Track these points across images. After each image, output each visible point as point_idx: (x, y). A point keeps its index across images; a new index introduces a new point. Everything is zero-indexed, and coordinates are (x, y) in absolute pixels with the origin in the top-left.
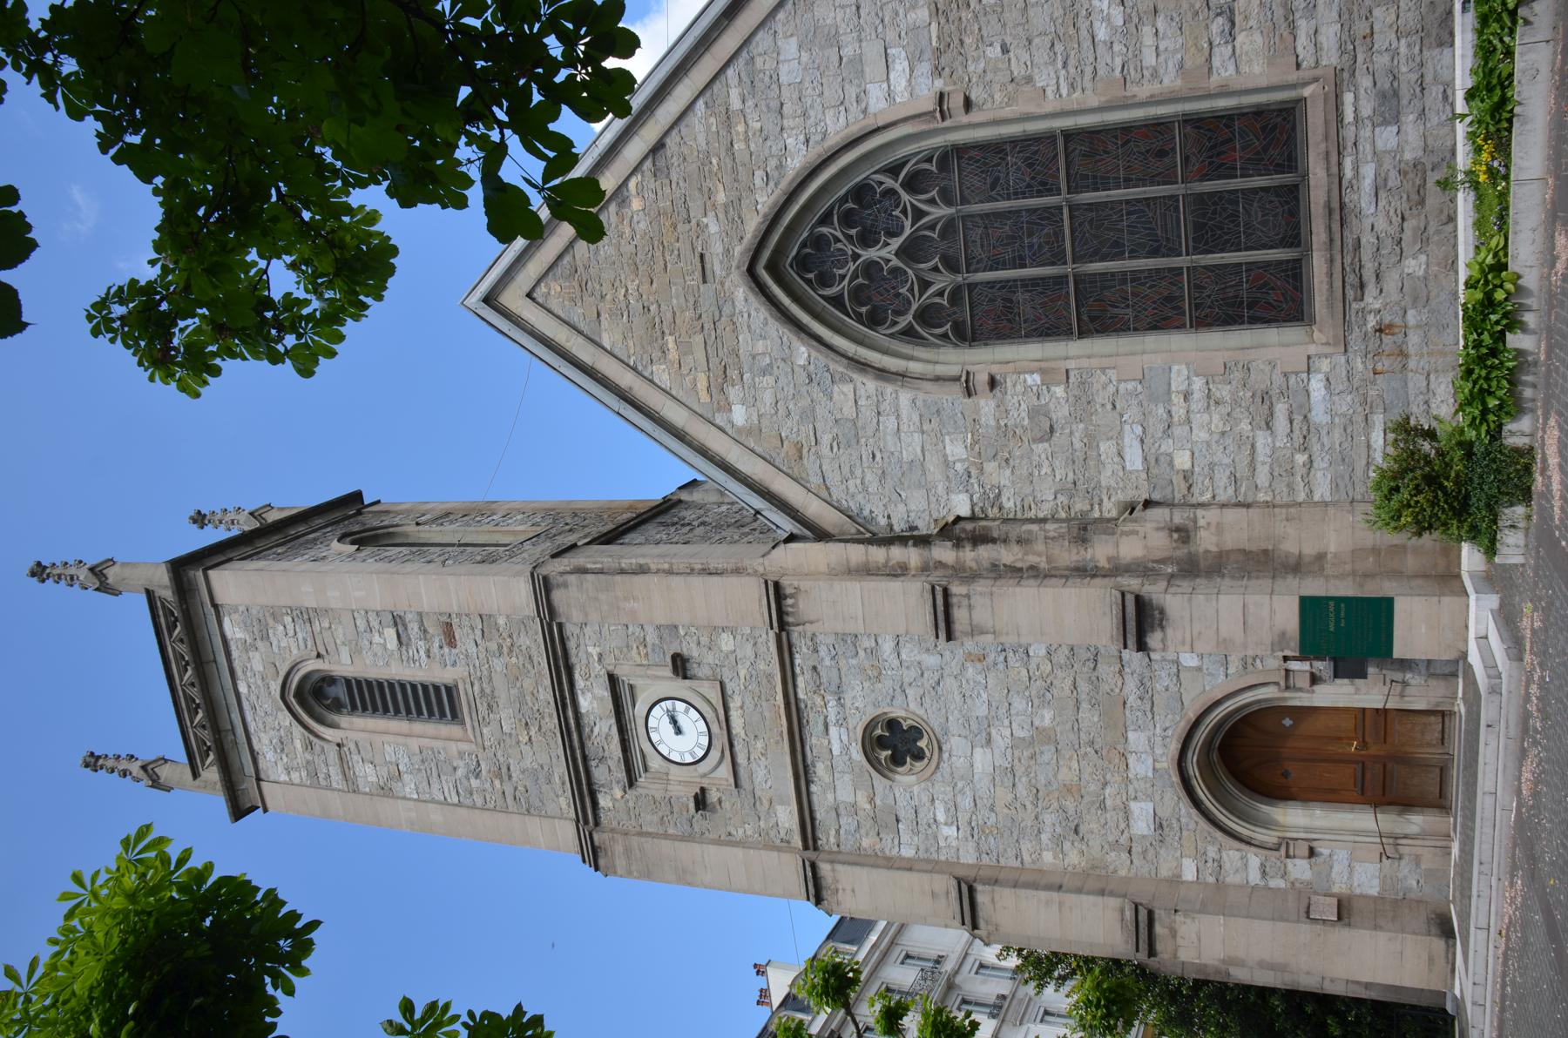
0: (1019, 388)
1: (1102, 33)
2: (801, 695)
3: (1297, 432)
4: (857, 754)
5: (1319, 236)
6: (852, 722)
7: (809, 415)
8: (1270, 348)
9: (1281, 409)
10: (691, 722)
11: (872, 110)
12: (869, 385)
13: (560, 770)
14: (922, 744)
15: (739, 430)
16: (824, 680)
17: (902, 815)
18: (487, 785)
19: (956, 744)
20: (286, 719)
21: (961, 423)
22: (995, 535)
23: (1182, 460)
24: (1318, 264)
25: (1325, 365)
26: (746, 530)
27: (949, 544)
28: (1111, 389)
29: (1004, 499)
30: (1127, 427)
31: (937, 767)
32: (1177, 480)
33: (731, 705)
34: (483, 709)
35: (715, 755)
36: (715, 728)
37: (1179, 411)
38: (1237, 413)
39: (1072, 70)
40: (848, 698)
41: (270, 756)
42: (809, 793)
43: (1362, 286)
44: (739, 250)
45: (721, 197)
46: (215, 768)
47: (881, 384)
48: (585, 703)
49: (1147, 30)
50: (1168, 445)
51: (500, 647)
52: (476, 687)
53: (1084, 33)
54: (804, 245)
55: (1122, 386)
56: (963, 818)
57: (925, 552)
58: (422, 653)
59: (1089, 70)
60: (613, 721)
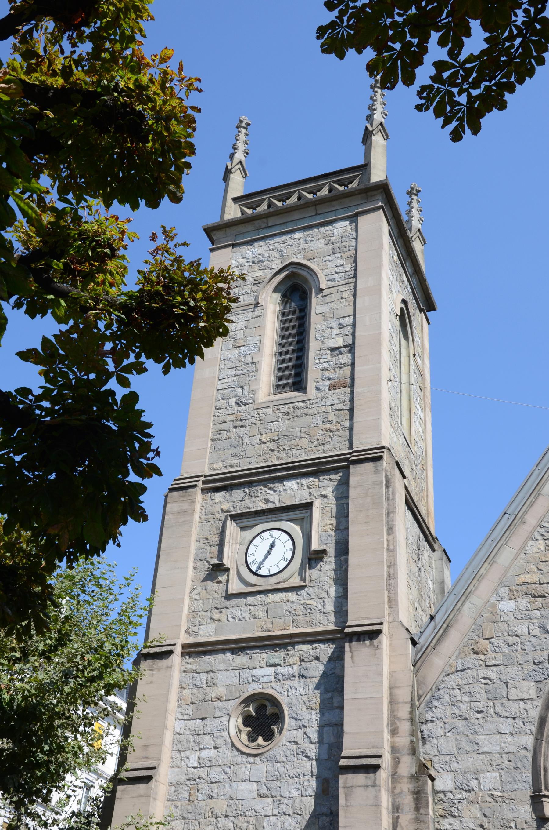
2: (297, 647)
4: (254, 688)
6: (278, 686)
10: (274, 563)
13: (244, 465)
14: (260, 740)
15: (494, 606)
16: (308, 665)
17: (207, 722)
18: (230, 411)
19: (261, 767)
20: (277, 265)
21: (509, 787)
22: (422, 811)
26: (416, 604)
27: (413, 771)
29: (451, 820)
31: (242, 753)
33: (289, 594)
34: (285, 409)
35: (252, 579)
36: (273, 580)
40: (295, 683)
41: (250, 254)
42: (223, 651)
46: (239, 214)
47: (536, 721)
48: (291, 484)
51: (330, 422)
52: (301, 404)
56: (202, 772)
57: (406, 751)
58: (325, 365)
60: (278, 505)
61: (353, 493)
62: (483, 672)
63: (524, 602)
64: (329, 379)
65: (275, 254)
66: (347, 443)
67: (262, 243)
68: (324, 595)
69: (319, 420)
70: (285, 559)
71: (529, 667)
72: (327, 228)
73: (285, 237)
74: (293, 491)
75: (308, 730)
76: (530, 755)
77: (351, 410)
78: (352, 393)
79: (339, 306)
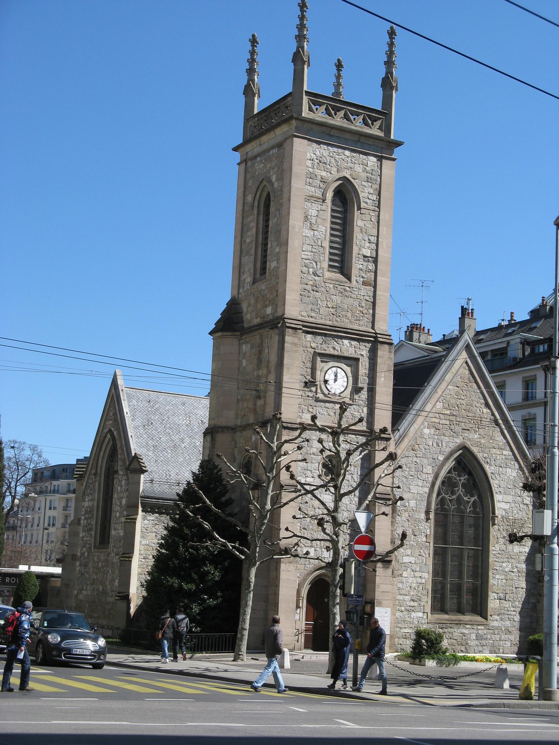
0: (426, 527)
1: (504, 565)
3: (410, 608)
5: (454, 617)
7: (424, 456)
8: (427, 602)
9: (416, 604)
11: (497, 495)
12: (430, 479)
15: (422, 430)
23: (405, 574)
24: (446, 616)
25: (425, 617)
28: (424, 555)
30: (414, 558)
32: (400, 572)
37: (417, 574)
38: (415, 591)
39: (497, 555)
43: (442, 628)
44: (468, 444)
45: (483, 441)
47: (431, 482)
49: (503, 577)
50: (409, 570)
52: (348, 289)
53: (505, 560)
54: (465, 464)
55: (424, 558)
59: (497, 560)
61: (379, 360)
62: (415, 459)
63: (433, 430)
64: (363, 277)
65: (333, 160)
66: (370, 323)
67: (325, 147)
68: (361, 411)
69: (356, 303)
70: (343, 386)
71: (431, 460)
72: (364, 157)
73: (340, 150)
74: (347, 347)
75: (353, 476)
76: (427, 495)
77: (374, 303)
78: (375, 292)
79: (370, 226)
